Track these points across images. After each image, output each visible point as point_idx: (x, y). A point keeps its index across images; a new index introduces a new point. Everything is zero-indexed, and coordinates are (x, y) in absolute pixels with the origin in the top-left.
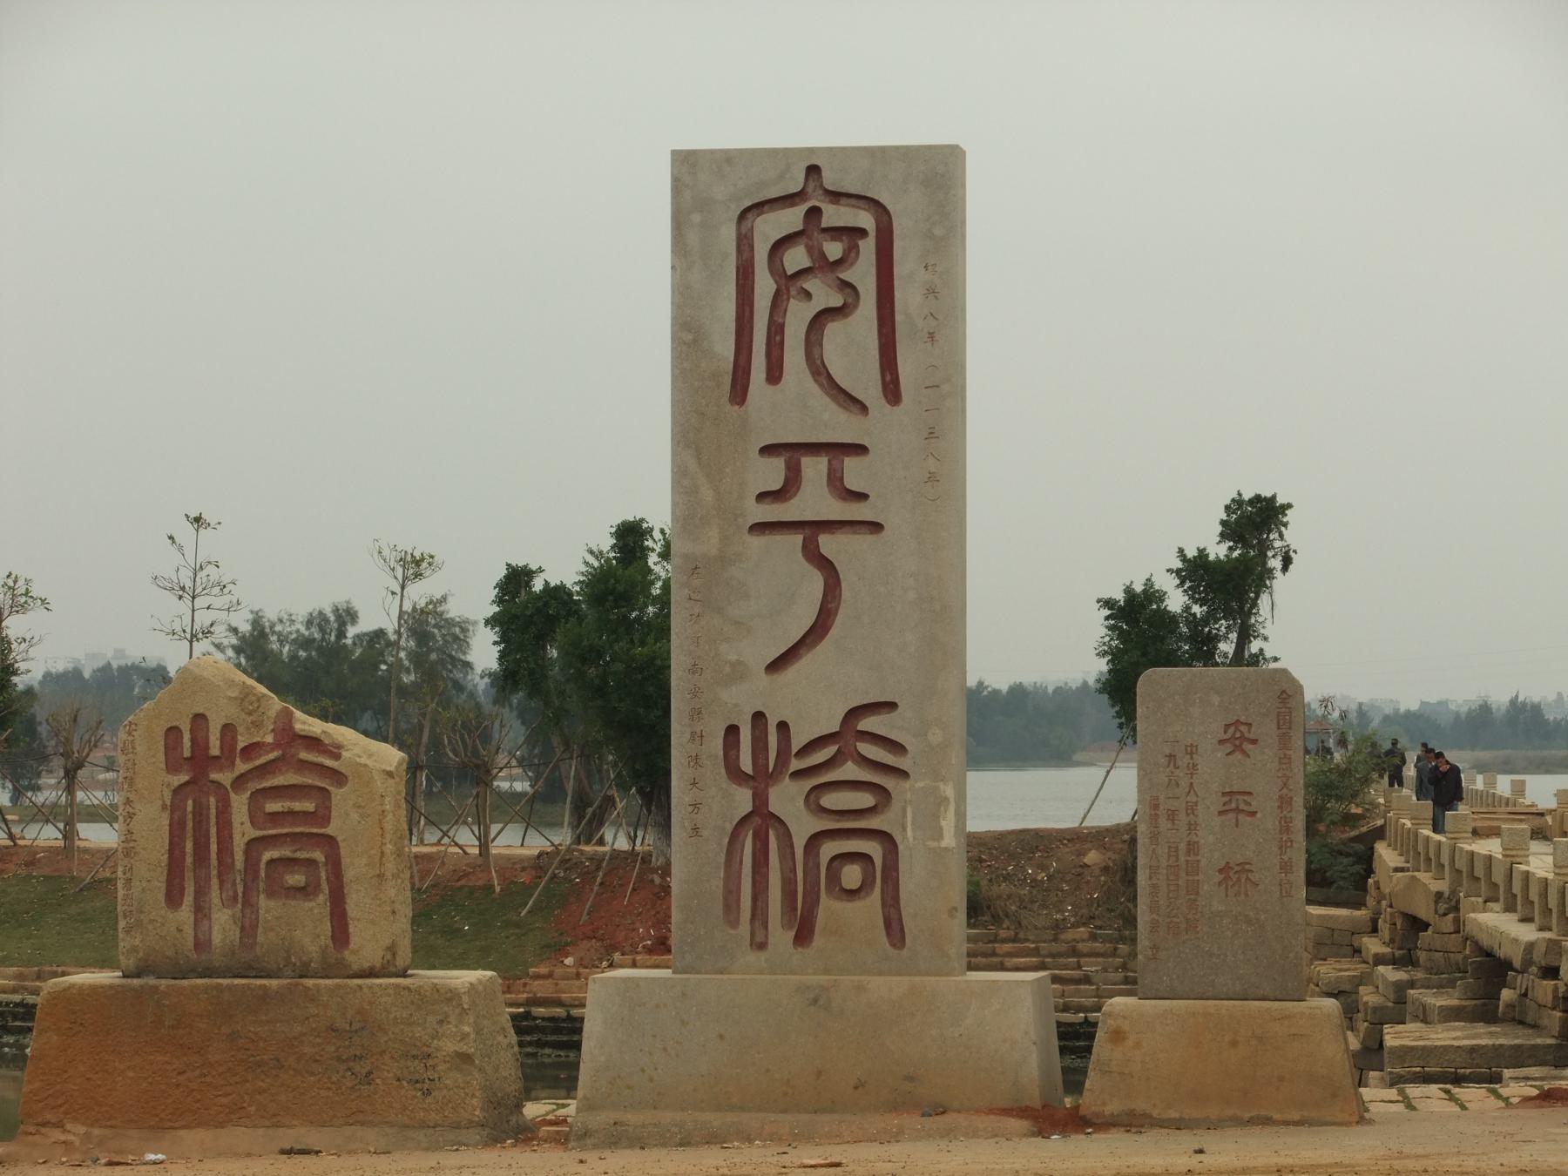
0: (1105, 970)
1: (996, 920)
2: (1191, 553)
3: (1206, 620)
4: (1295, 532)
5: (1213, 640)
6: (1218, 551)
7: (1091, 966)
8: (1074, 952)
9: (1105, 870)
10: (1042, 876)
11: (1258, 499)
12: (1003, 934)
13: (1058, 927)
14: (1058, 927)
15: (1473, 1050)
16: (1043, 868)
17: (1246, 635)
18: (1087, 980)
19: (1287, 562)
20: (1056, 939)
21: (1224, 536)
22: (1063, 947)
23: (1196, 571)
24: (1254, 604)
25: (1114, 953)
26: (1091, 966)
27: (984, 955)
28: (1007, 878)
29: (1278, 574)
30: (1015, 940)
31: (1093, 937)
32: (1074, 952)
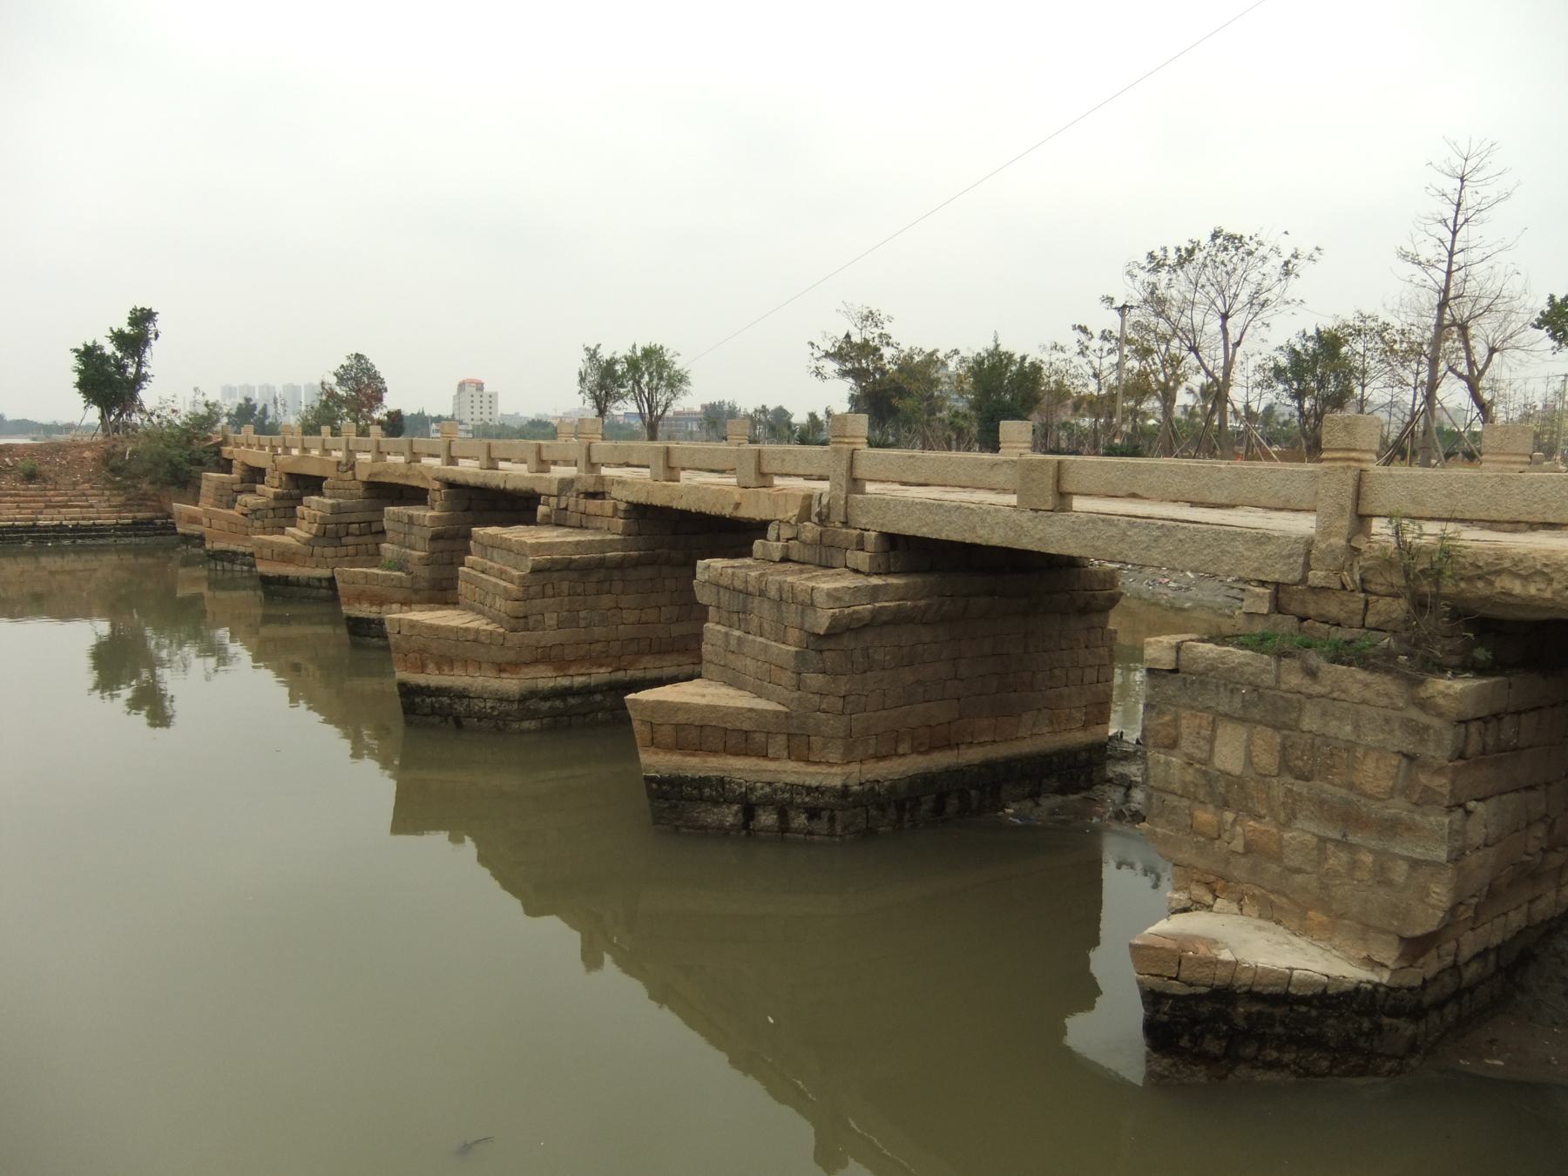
0: (100, 502)
1: (45, 481)
2: (115, 330)
3: (122, 359)
4: (160, 324)
5: (125, 367)
6: (127, 329)
7: (93, 501)
8: (84, 495)
9: (94, 459)
10: (64, 462)
11: (143, 309)
12: (49, 487)
13: (75, 484)
14: (75, 484)
15: (578, 543)
16: (65, 459)
17: (140, 365)
18: (92, 506)
19: (157, 336)
20: (74, 489)
21: (130, 324)
22: (74, 493)
23: (119, 338)
24: (144, 352)
25: (103, 495)
26: (93, 501)
27: (41, 496)
28: (47, 463)
29: (153, 342)
30: (55, 489)
31: (92, 488)
32: (84, 495)
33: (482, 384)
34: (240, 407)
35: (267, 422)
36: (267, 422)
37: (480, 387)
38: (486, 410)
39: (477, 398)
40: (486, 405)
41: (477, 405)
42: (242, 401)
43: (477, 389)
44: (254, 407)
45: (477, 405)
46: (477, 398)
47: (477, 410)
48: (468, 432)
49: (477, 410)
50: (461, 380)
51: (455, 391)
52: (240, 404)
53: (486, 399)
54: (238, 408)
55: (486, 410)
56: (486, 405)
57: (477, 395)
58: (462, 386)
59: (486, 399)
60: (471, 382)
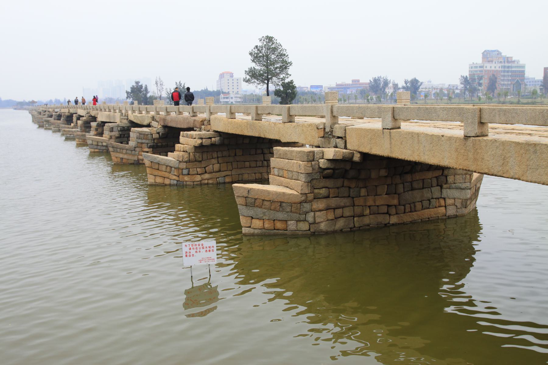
33: (233, 74)
34: (133, 89)
35: (148, 95)
36: (148, 95)
37: (232, 75)
38: (235, 87)
39: (231, 81)
40: (235, 84)
41: (231, 84)
42: (134, 84)
43: (231, 77)
44: (141, 86)
45: (231, 84)
46: (231, 81)
47: (231, 87)
48: (240, 98)
49: (231, 87)
50: (221, 73)
51: (217, 78)
52: (133, 86)
53: (235, 81)
54: (131, 88)
55: (235, 87)
56: (235, 84)
57: (231, 79)
58: (222, 76)
59: (235, 81)
60: (227, 73)
